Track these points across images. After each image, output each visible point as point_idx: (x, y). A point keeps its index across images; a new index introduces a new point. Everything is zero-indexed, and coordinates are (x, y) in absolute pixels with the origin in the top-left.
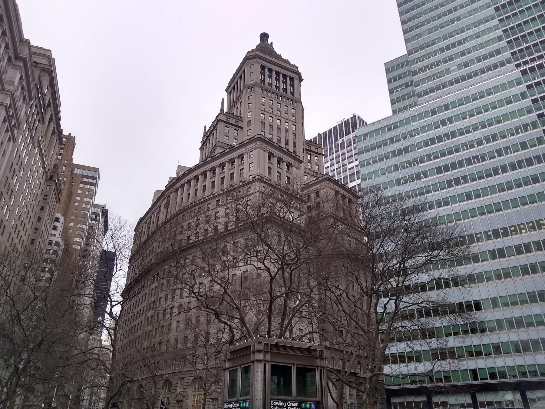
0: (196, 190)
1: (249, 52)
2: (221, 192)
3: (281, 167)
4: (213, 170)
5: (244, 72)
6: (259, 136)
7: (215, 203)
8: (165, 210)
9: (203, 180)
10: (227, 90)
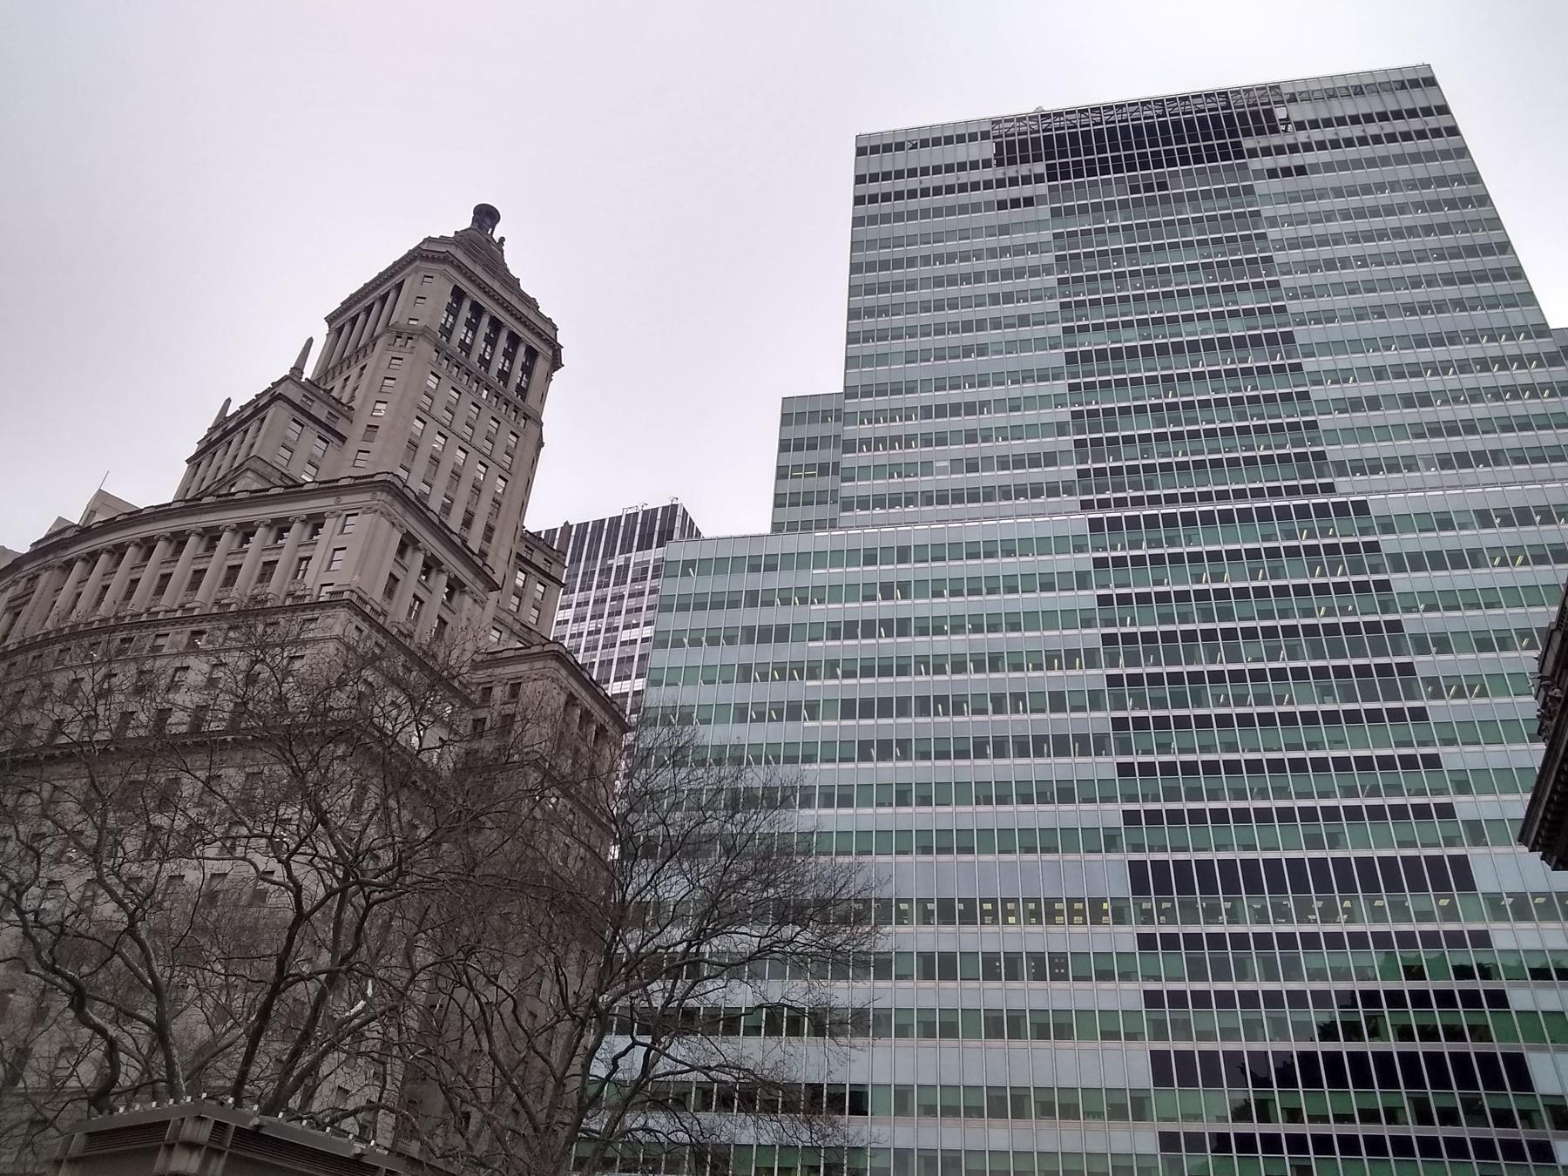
0: (135, 582)
1: (429, 240)
2: (215, 610)
3: (431, 584)
4: (211, 537)
5: (399, 287)
6: (390, 477)
7: (185, 639)
9: (168, 556)
10: (330, 319)
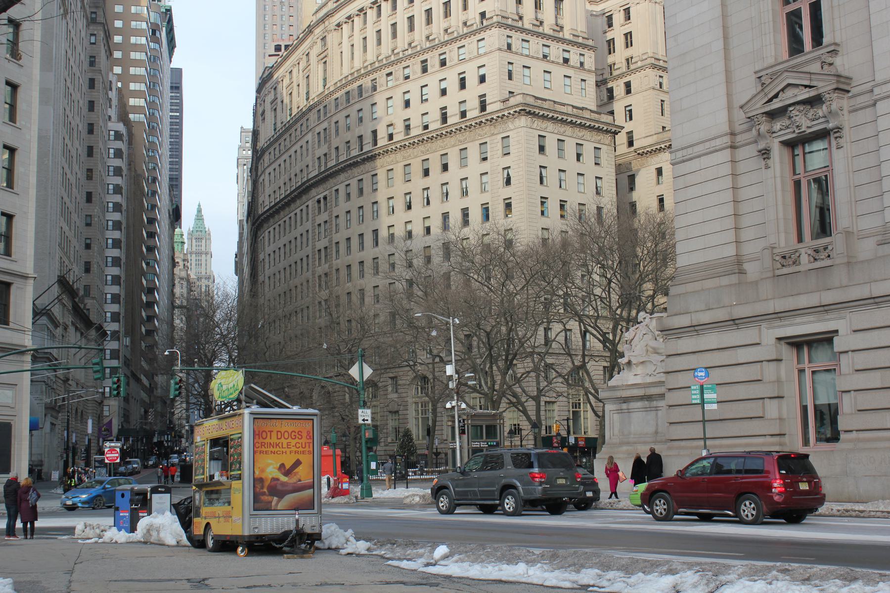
0: (379, 32)
7: (418, 68)
8: (321, 66)
